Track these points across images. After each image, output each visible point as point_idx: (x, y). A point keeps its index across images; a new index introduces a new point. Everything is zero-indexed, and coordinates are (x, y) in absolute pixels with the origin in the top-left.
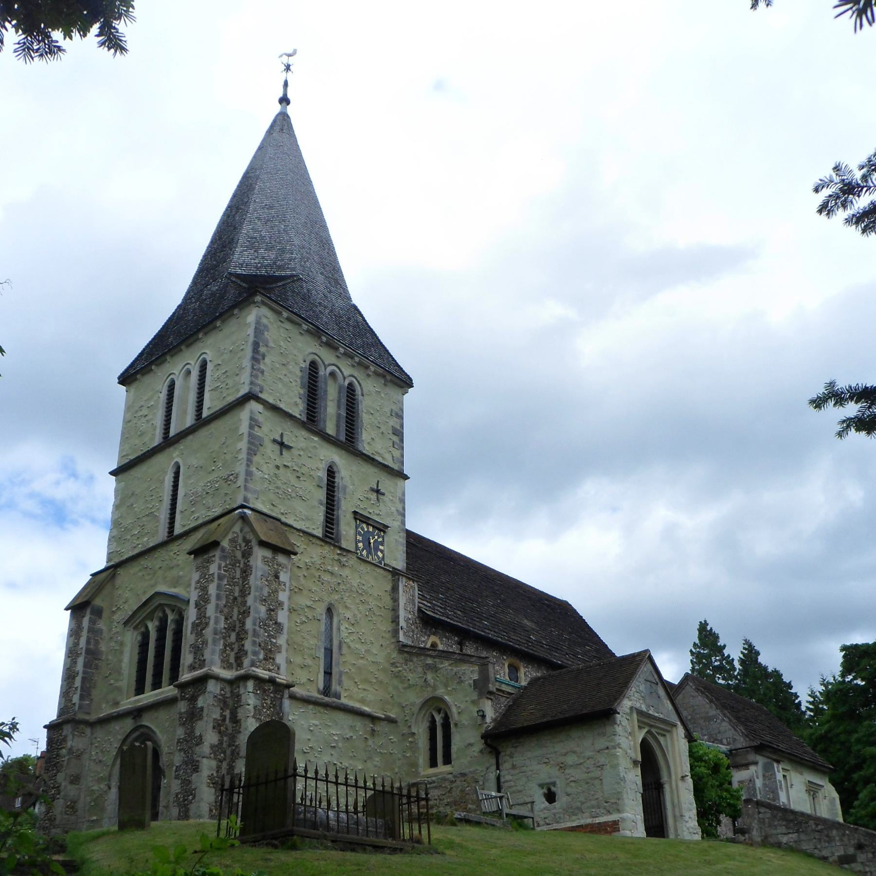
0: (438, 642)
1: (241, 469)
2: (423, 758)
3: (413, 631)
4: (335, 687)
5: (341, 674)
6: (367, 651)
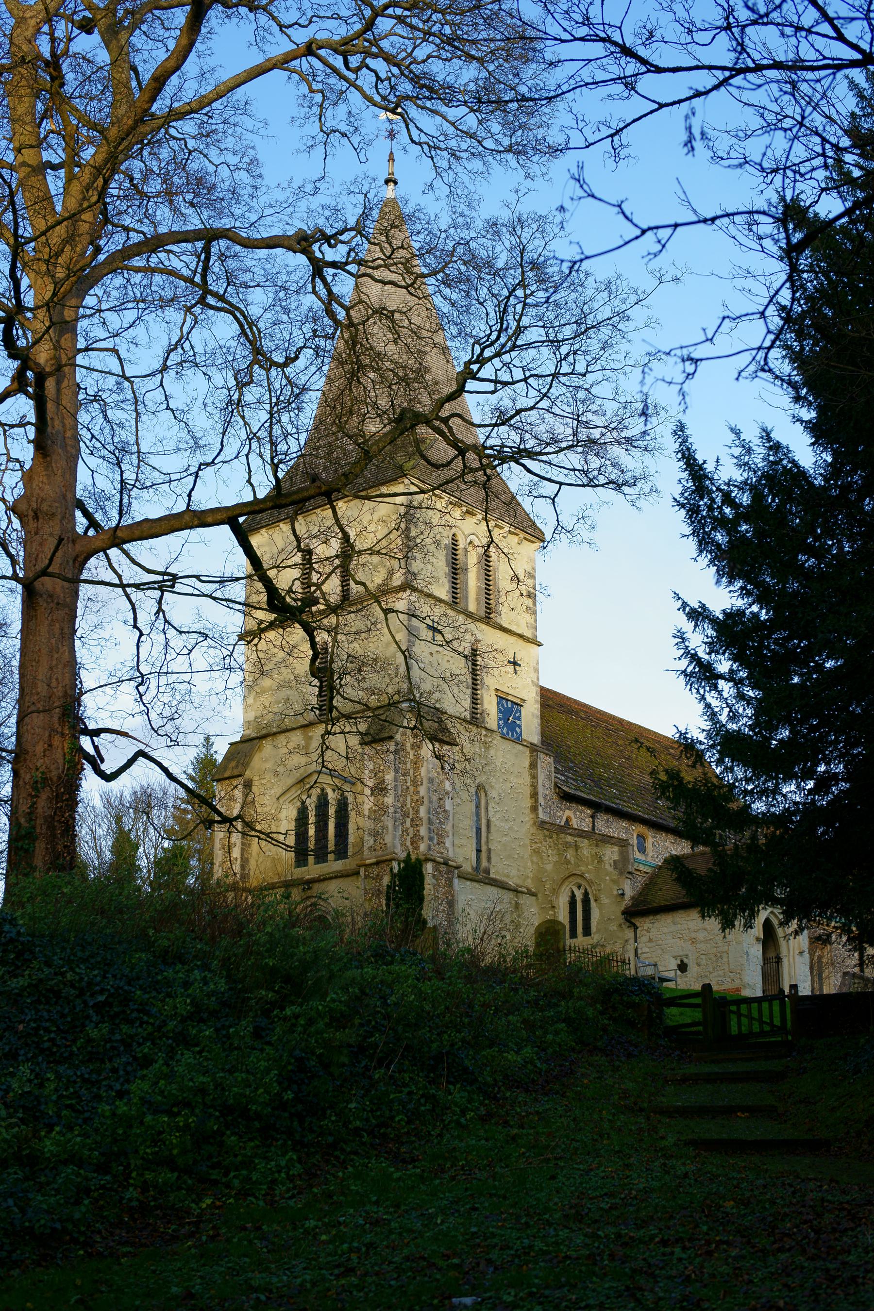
0: (572, 816)
4: (484, 863)
6: (510, 828)
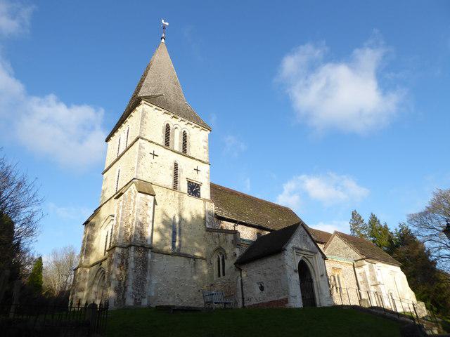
1: (136, 165)
2: (216, 273)
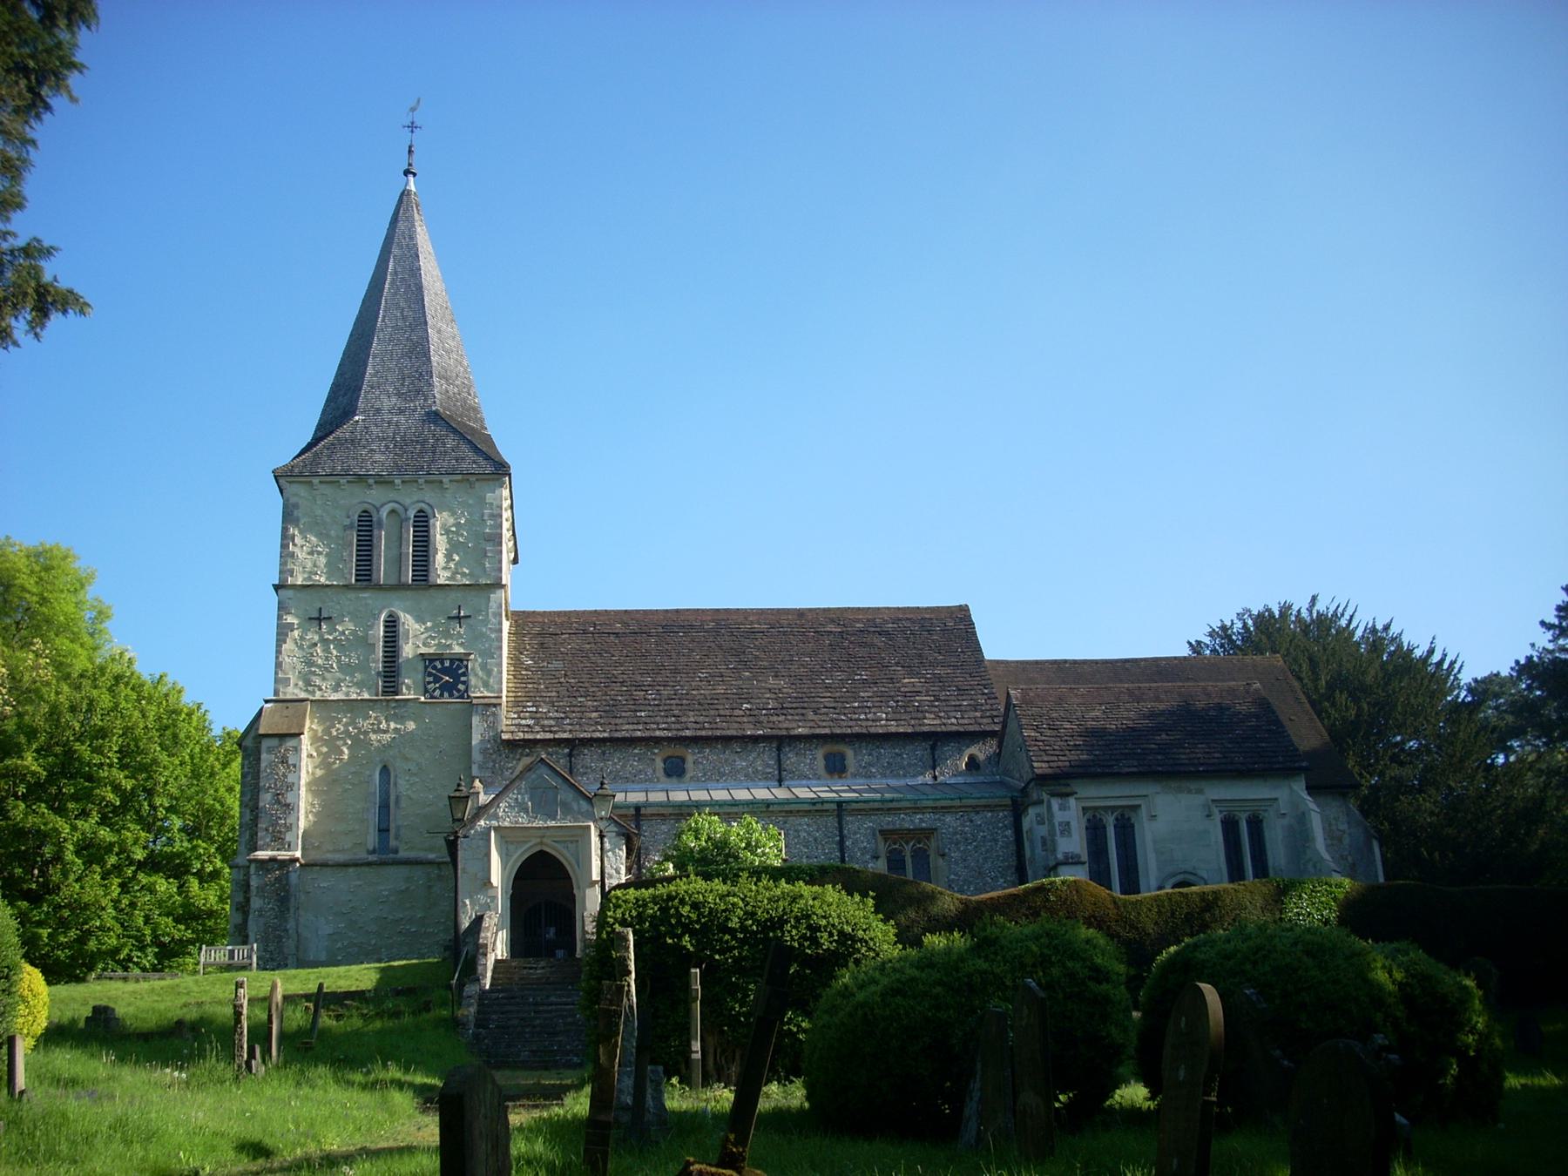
3: (494, 761)
5: (398, 828)
